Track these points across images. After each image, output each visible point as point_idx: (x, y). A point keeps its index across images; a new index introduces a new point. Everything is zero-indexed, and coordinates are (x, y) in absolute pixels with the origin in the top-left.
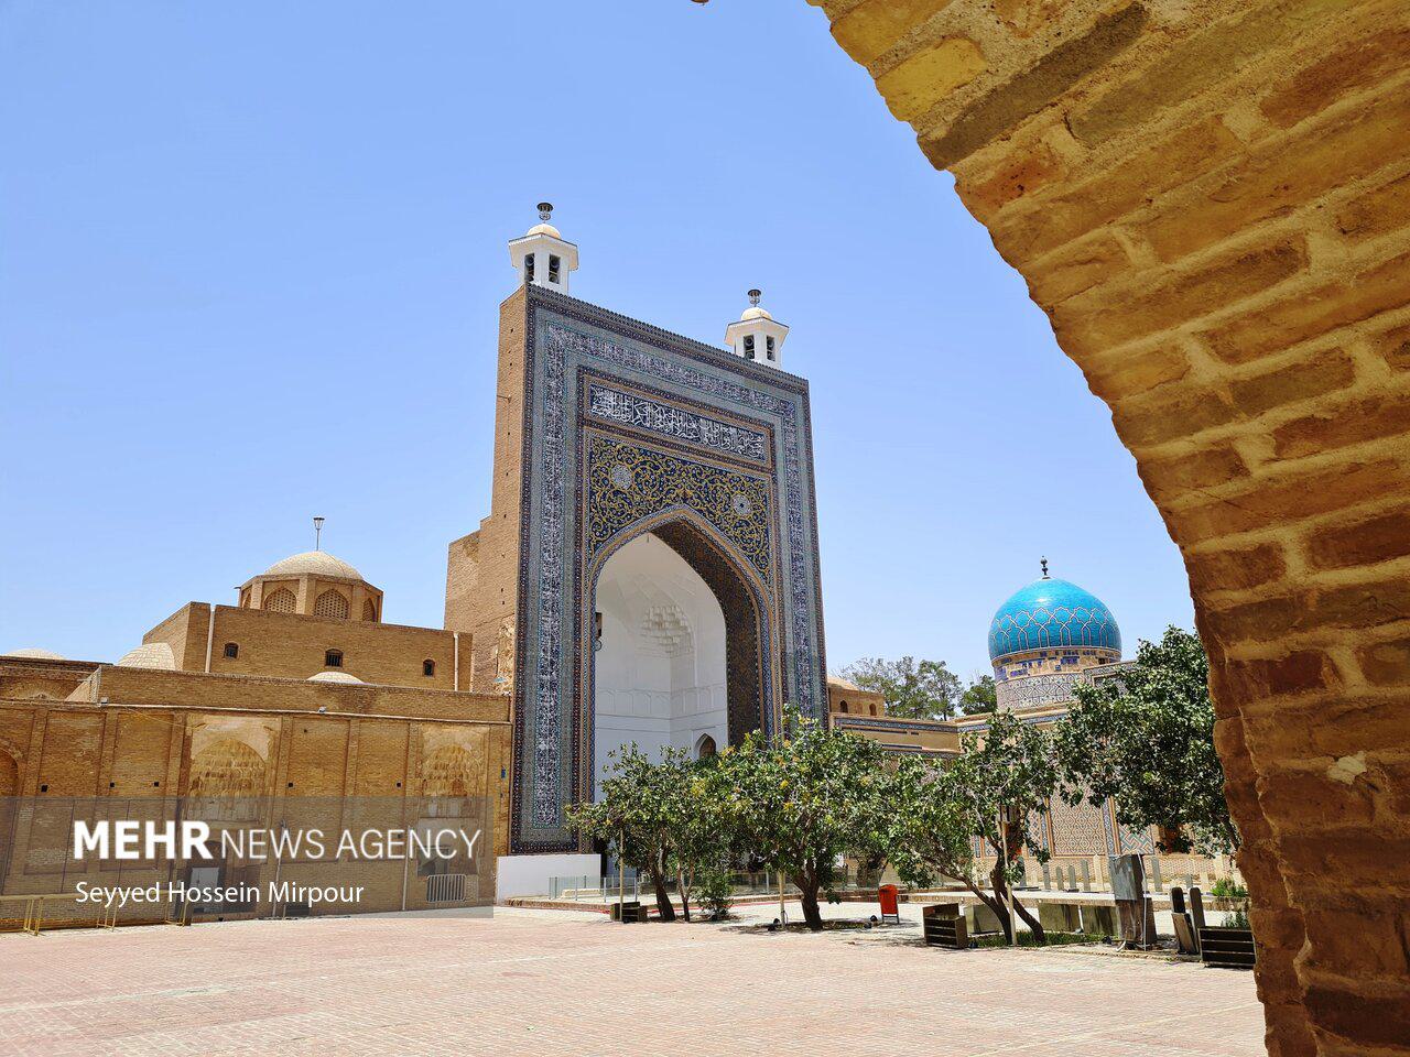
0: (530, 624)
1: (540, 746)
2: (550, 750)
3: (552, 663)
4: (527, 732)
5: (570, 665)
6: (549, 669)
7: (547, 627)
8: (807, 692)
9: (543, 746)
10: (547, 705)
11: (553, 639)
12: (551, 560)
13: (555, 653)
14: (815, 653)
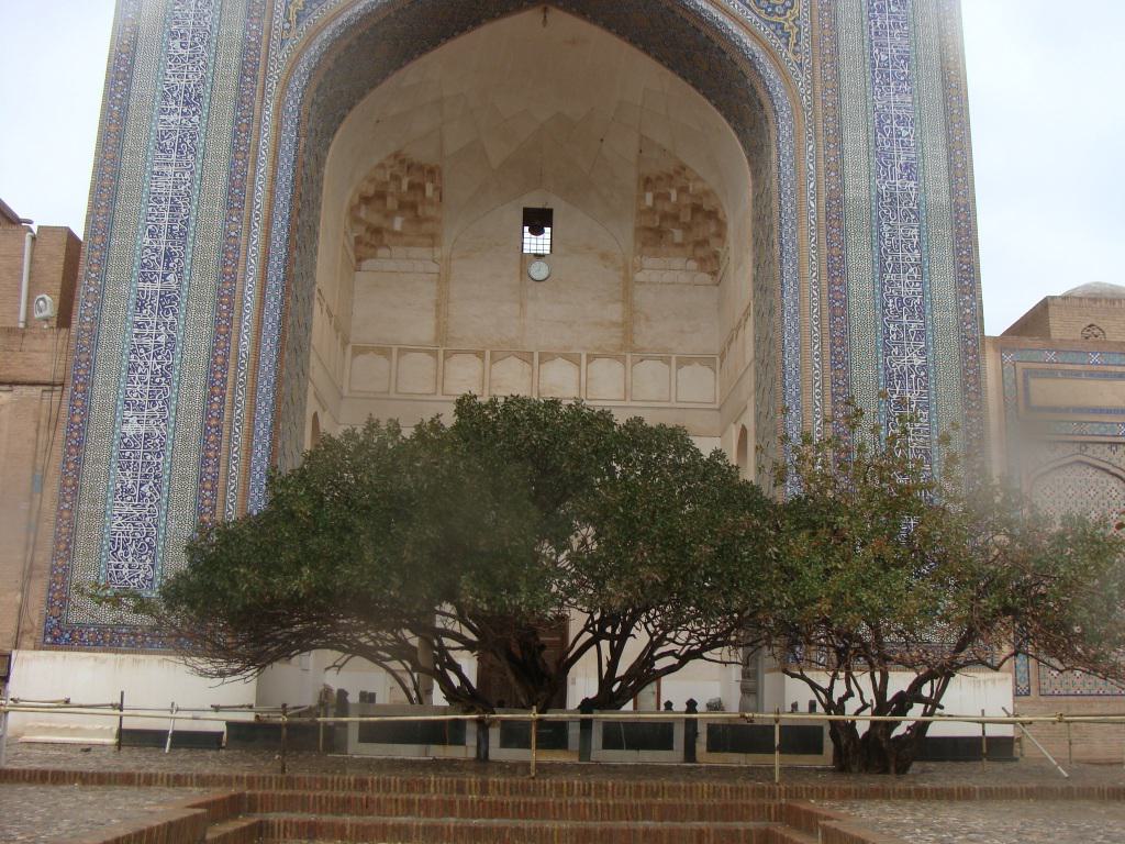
0: (124, 182)
1: (125, 428)
2: (148, 436)
3: (169, 256)
4: (96, 402)
5: (214, 257)
6: (160, 270)
7: (164, 186)
8: (906, 287)
9: (129, 430)
10: (151, 343)
11: (175, 208)
12: (186, 53)
13: (179, 236)
14: (939, 195)
